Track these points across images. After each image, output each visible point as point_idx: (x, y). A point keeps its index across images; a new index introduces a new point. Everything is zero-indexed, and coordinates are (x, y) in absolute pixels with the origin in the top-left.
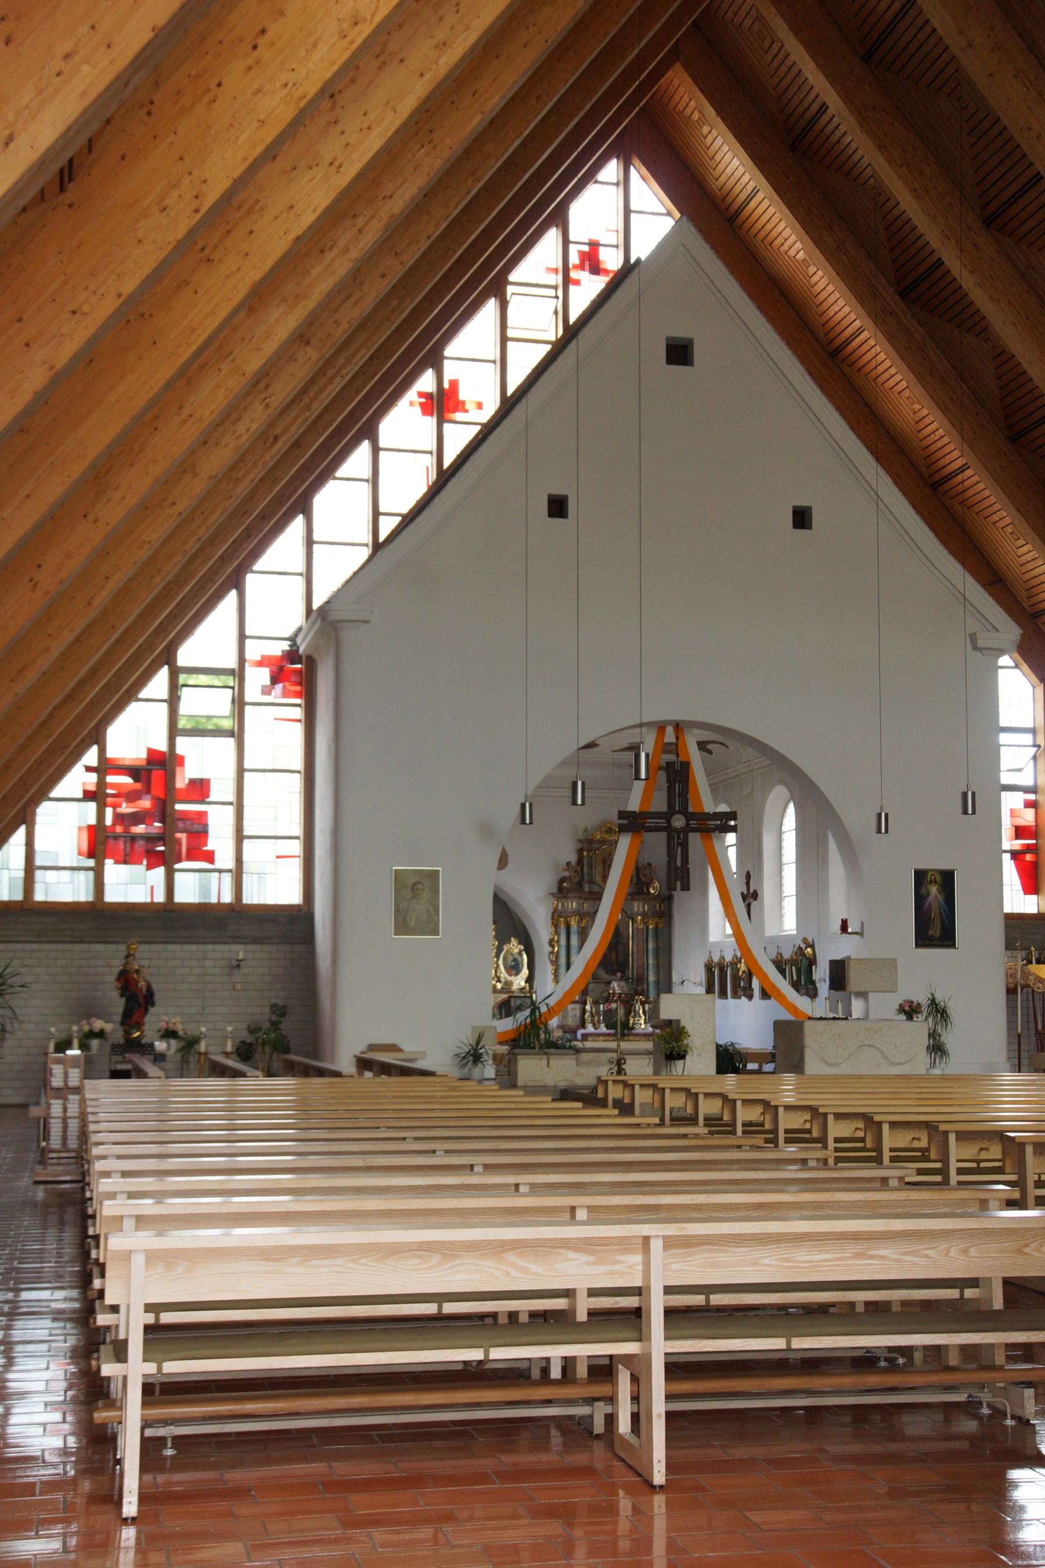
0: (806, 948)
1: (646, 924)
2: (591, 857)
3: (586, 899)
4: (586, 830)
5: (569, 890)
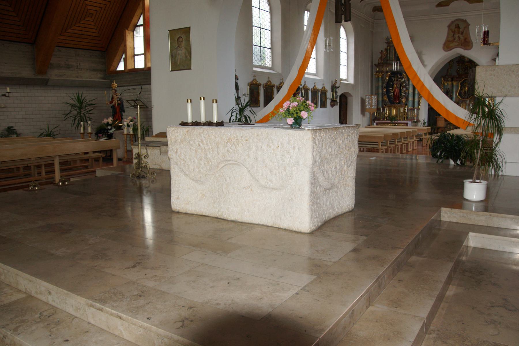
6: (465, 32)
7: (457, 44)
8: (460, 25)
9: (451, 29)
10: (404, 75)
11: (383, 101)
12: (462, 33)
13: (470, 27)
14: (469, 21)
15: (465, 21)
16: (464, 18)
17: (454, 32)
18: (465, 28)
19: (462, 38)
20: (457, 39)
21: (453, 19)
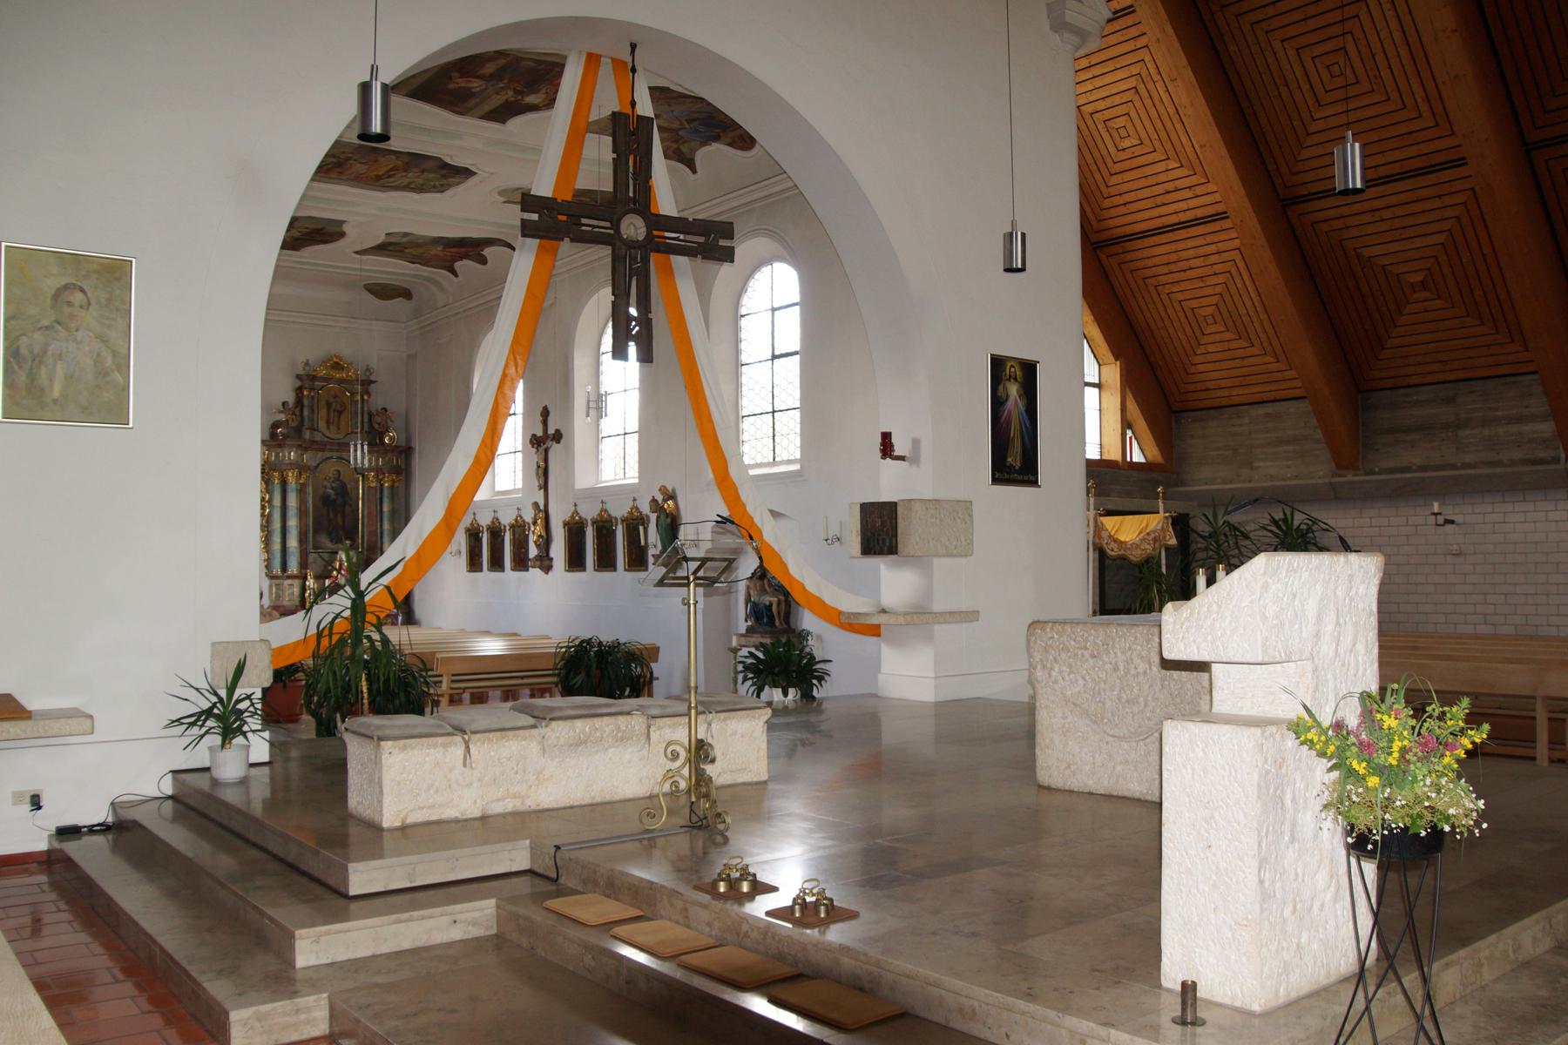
0: (665, 500)
1: (380, 482)
2: (313, 397)
3: (306, 449)
4: (307, 364)
5: (285, 436)
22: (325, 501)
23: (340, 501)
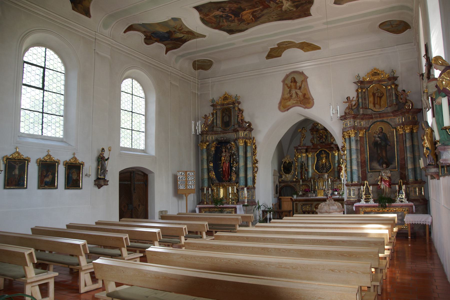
6: (303, 86)
7: (295, 102)
8: (296, 79)
9: (286, 84)
10: (232, 144)
11: (210, 178)
12: (300, 88)
13: (308, 80)
14: (306, 73)
15: (302, 73)
16: (300, 70)
17: (290, 88)
18: (302, 82)
19: (300, 94)
20: (294, 95)
21: (288, 72)
22: (376, 144)
23: (383, 143)
